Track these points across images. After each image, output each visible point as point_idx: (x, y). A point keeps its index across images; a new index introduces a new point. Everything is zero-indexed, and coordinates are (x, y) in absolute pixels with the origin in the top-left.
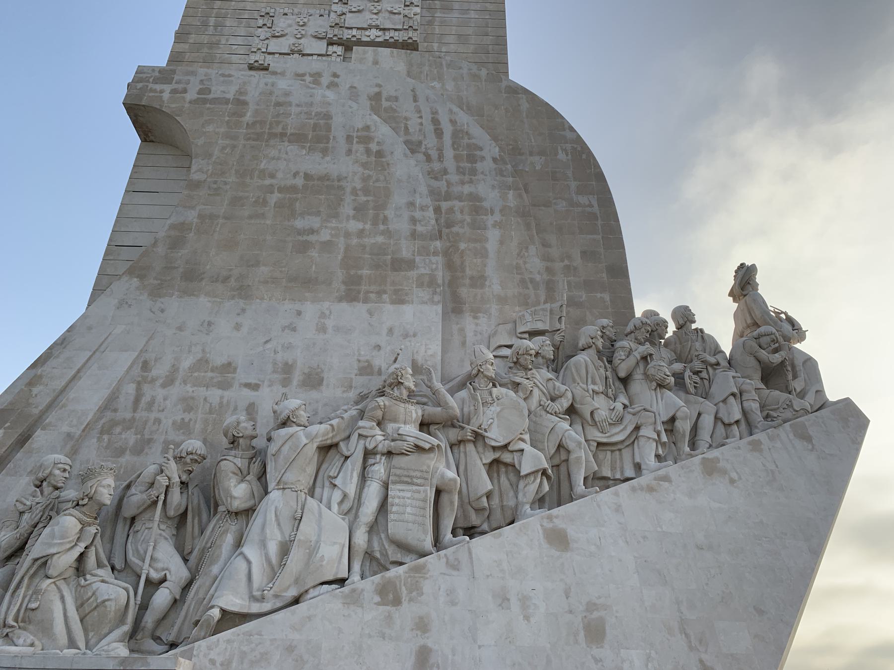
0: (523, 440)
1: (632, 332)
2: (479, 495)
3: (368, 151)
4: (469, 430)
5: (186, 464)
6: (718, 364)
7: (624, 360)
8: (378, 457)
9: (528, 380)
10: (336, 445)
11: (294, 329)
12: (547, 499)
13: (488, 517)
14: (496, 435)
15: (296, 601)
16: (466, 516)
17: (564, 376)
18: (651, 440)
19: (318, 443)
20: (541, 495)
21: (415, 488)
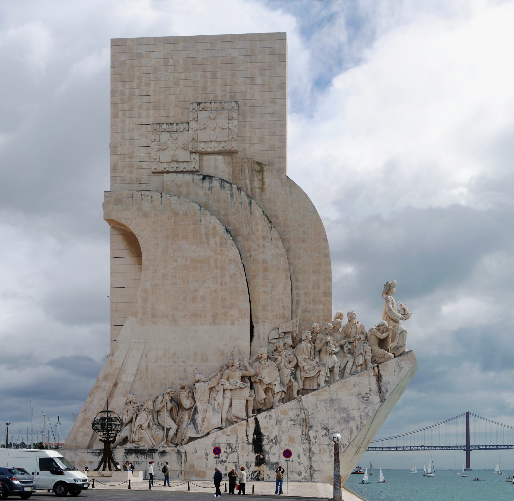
0: (277, 380)
2: (261, 399)
3: (216, 244)
4: (258, 379)
5: (170, 394)
6: (360, 339)
8: (228, 391)
9: (281, 357)
10: (215, 387)
11: (195, 338)
12: (285, 398)
13: (265, 405)
14: (267, 380)
15: (208, 434)
16: (257, 406)
17: (296, 351)
19: (209, 388)
20: (282, 398)
21: (240, 400)
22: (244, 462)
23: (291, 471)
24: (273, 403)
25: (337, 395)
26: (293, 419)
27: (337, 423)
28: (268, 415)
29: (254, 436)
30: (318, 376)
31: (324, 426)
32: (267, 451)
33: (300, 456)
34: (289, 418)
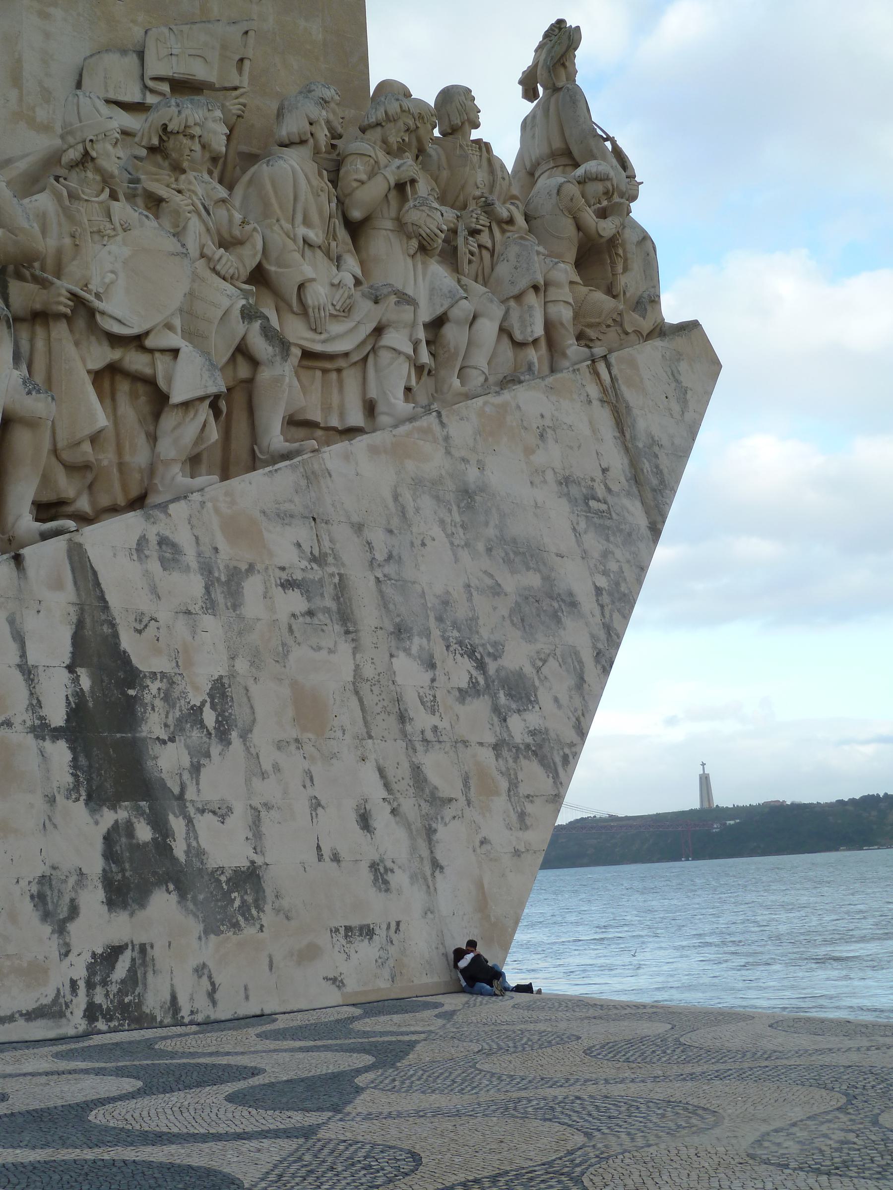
0: (169, 327)
1: (378, 124)
4: (64, 292)
6: (511, 221)
7: (363, 183)
12: (205, 457)
18: (402, 358)
22: (23, 883)
23: (337, 930)
24: (152, 470)
25: (481, 467)
26: (298, 576)
27: (513, 624)
28: (153, 539)
29: (76, 680)
30: (365, 359)
31: (456, 634)
32: (176, 790)
33: (371, 822)
34: (279, 573)
